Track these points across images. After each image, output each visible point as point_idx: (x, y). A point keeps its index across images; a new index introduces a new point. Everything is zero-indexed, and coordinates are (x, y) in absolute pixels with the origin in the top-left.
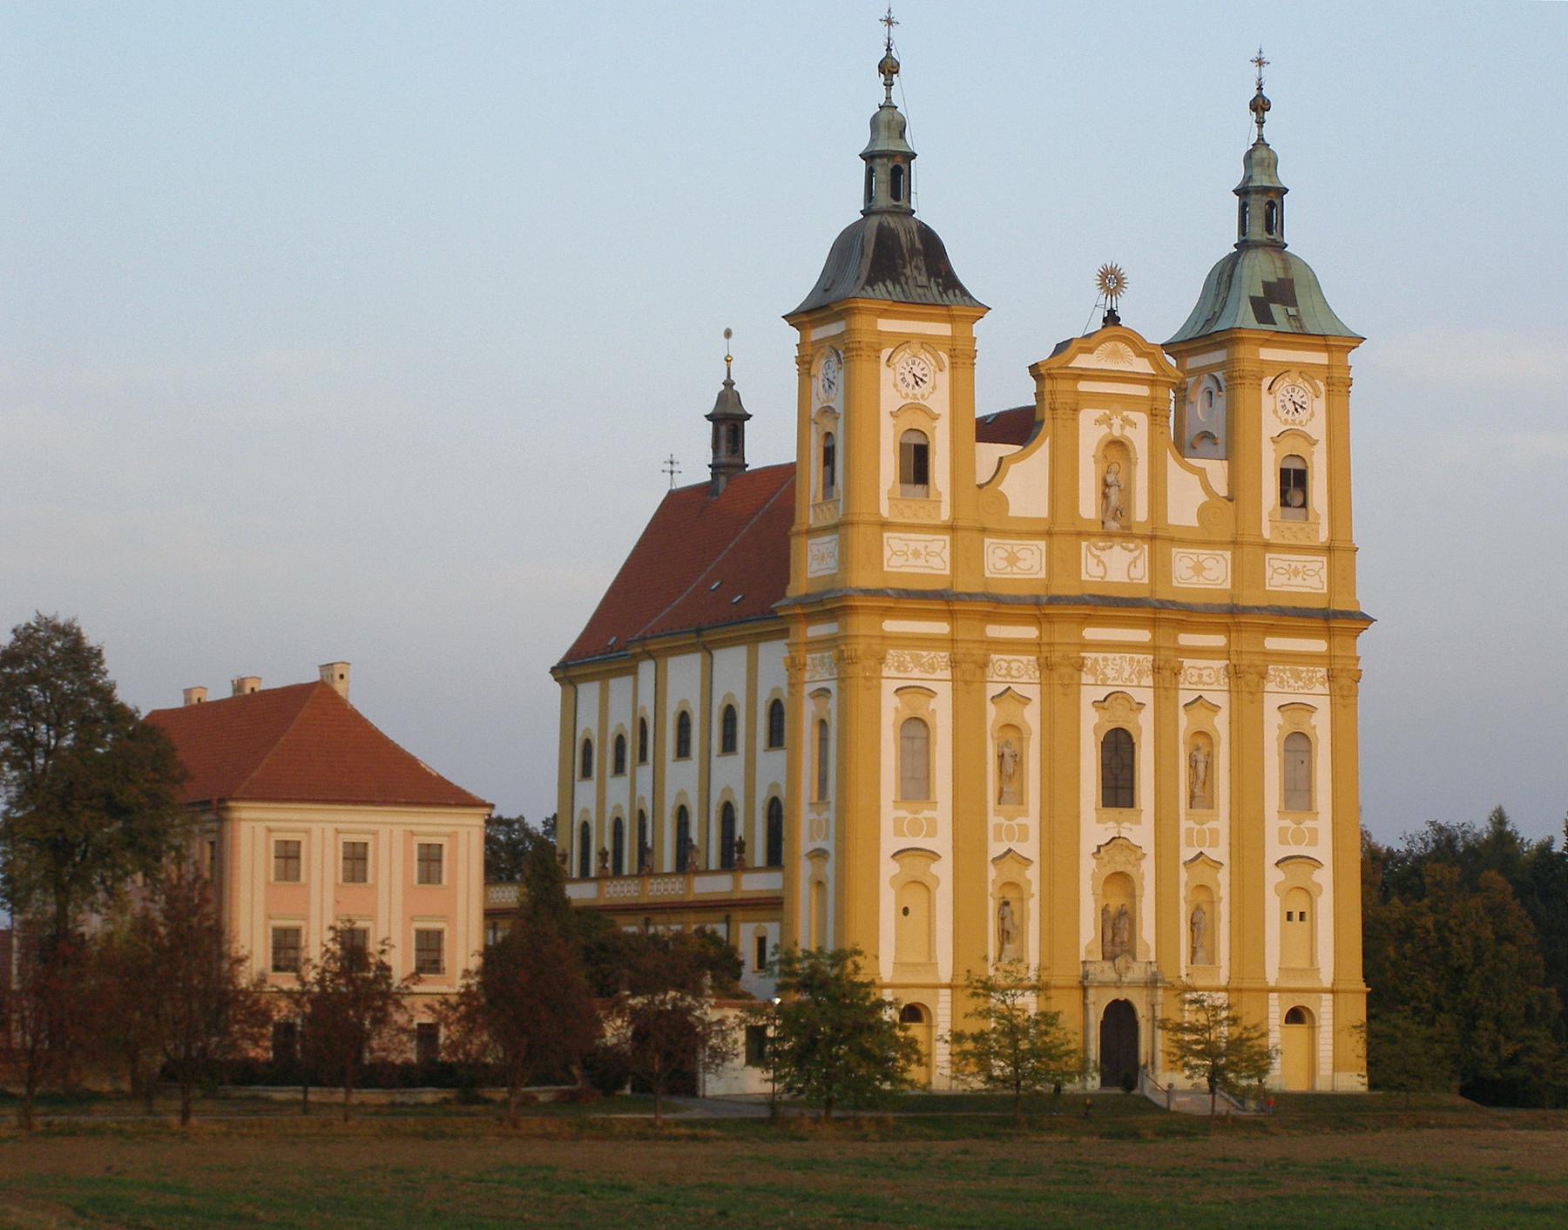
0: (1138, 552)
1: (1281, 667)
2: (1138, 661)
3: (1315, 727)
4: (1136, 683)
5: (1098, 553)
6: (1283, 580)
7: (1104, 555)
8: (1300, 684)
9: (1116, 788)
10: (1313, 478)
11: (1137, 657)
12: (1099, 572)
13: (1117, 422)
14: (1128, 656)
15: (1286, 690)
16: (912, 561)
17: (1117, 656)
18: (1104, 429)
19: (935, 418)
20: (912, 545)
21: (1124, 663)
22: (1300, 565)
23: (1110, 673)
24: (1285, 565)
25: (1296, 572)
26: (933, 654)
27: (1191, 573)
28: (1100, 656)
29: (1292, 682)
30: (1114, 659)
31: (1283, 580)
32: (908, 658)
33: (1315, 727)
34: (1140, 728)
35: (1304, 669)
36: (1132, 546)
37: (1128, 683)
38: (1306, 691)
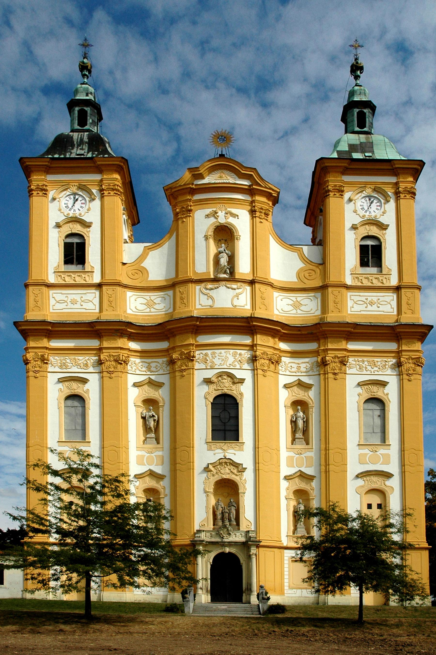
0: (240, 291)
1: (360, 359)
2: (240, 354)
3: (387, 394)
4: (238, 367)
5: (208, 291)
6: (363, 307)
7: (212, 293)
8: (376, 369)
9: (225, 430)
10: (385, 248)
11: (239, 352)
12: (210, 302)
13: (221, 214)
14: (232, 351)
15: (365, 372)
16: (70, 305)
17: (223, 351)
18: (212, 220)
19: (88, 225)
20: (71, 297)
21: (228, 355)
22: (375, 299)
23: (217, 361)
24: (363, 299)
25: (371, 303)
26: (87, 358)
27: (291, 308)
28: (209, 352)
29: (369, 368)
30: (221, 353)
31: (363, 307)
32: (68, 361)
33: (387, 394)
34: (241, 394)
35: (379, 360)
36: (234, 286)
37: (232, 367)
38: (380, 373)
